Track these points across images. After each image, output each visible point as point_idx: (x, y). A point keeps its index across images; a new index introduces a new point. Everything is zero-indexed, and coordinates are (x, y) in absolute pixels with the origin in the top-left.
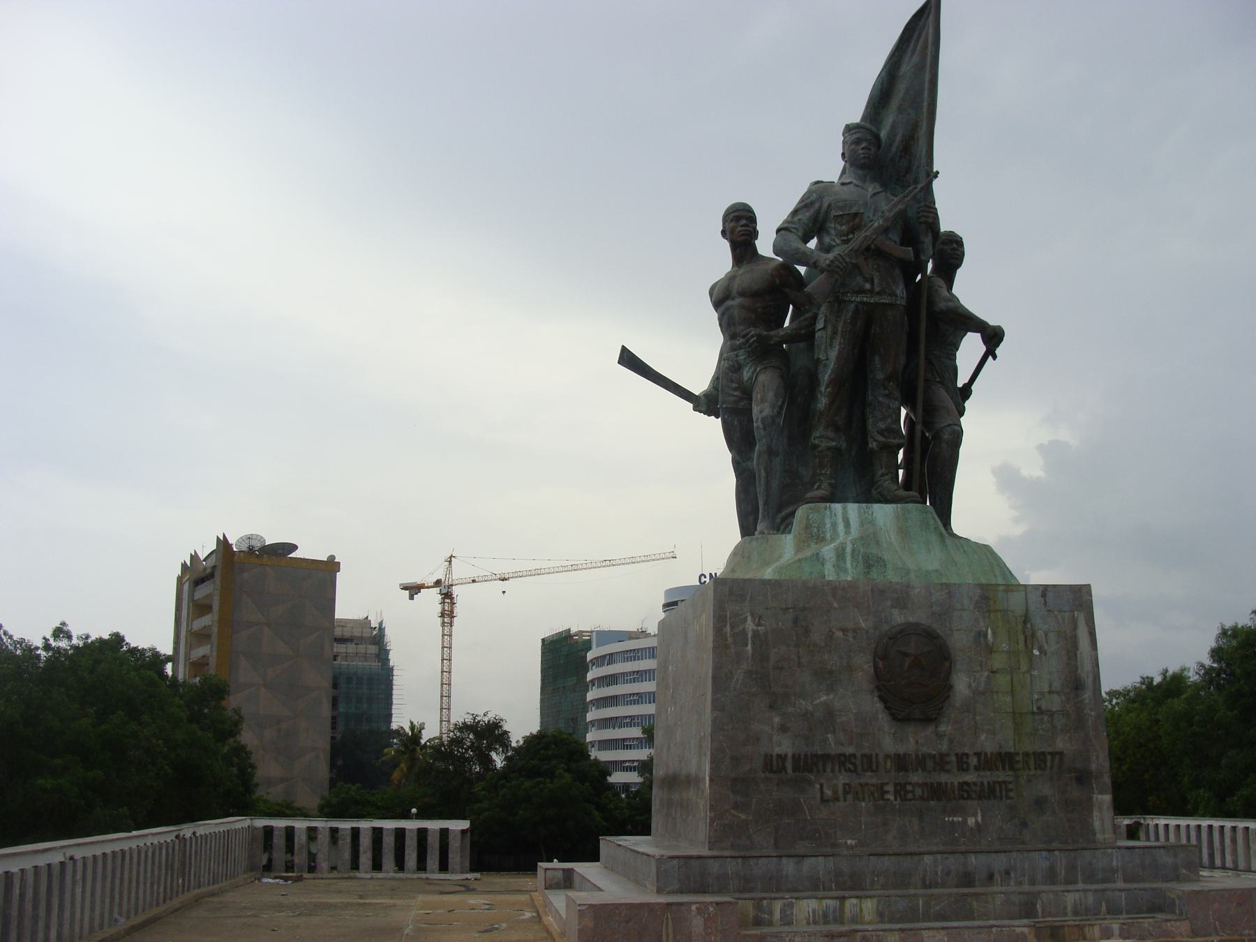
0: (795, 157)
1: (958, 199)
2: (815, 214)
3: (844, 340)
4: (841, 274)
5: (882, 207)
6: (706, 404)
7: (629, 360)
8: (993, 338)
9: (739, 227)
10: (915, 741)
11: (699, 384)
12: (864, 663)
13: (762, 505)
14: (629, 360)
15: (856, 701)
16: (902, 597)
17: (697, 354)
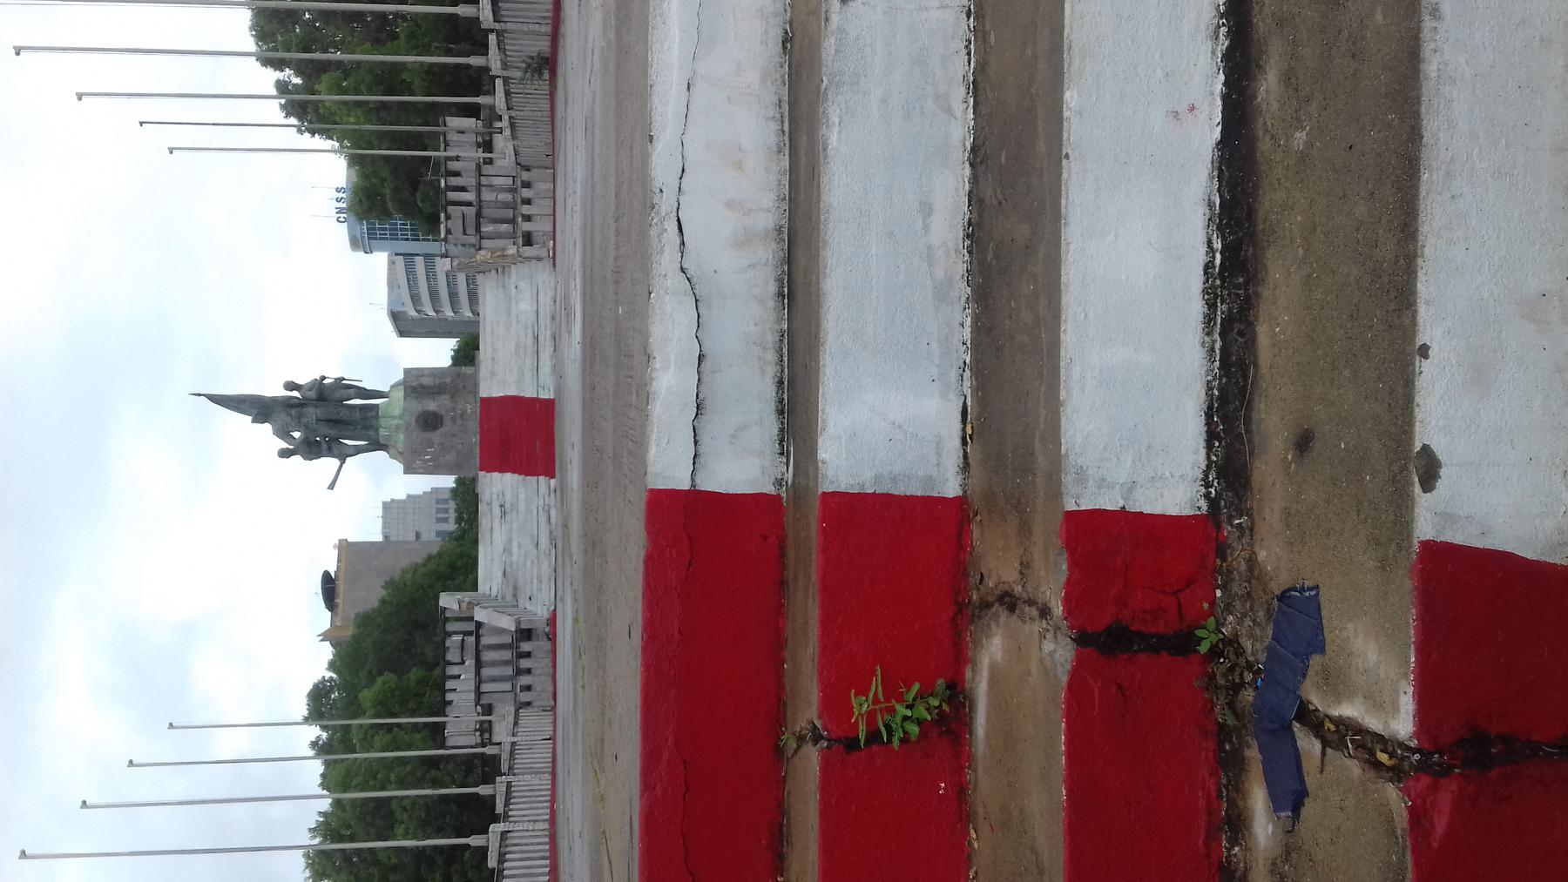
1: (276, 390)
2: (283, 433)
3: (322, 420)
4: (306, 428)
5: (283, 417)
6: (343, 462)
7: (331, 487)
8: (324, 378)
9: (285, 454)
10: (447, 421)
11: (335, 462)
12: (426, 435)
13: (376, 445)
14: (331, 487)
15: (436, 436)
17: (328, 464)
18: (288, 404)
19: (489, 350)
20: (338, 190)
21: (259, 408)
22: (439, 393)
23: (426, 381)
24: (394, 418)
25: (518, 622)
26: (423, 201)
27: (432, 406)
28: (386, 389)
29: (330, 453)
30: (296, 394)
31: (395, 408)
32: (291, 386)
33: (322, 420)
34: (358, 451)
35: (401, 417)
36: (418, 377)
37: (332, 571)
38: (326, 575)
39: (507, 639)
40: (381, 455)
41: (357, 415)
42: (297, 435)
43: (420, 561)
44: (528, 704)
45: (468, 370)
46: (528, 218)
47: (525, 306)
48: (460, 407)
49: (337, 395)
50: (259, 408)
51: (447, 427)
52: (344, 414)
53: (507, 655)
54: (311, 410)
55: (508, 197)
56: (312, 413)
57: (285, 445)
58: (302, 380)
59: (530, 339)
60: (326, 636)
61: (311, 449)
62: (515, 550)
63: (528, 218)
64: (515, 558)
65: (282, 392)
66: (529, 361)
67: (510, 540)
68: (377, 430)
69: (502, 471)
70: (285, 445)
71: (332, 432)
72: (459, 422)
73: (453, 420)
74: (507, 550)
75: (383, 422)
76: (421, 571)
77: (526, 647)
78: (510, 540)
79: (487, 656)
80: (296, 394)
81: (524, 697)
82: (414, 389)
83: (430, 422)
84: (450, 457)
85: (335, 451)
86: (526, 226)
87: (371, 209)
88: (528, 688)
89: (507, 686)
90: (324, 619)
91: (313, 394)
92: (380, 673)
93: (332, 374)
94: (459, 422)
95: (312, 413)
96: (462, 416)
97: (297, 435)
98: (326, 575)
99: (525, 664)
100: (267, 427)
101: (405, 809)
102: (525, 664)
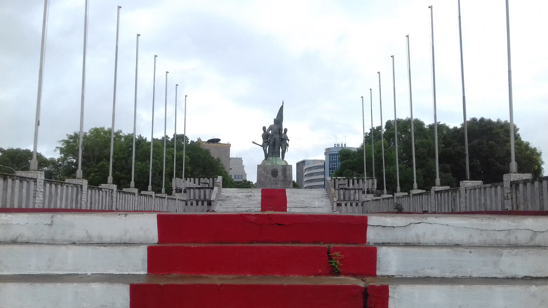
0: (269, 122)
1: (285, 125)
2: (271, 128)
3: (275, 140)
4: (272, 135)
5: (276, 128)
7: (253, 142)
8: (288, 140)
9: (264, 128)
10: (274, 179)
11: (261, 144)
12: (270, 172)
13: (267, 156)
14: (253, 142)
15: (270, 175)
16: (274, 166)
17: (261, 142)
18: (280, 129)
19: (301, 192)
20: (345, 144)
21: (279, 120)
22: (284, 176)
23: (288, 172)
24: (276, 162)
25: (213, 201)
26: (347, 172)
27: (280, 174)
28: (285, 159)
29: (264, 142)
30: (283, 132)
31: (279, 162)
32: (286, 130)
33: (275, 140)
34: (265, 151)
35: (276, 164)
36: (289, 169)
37: (220, 142)
38: (219, 140)
39: (207, 198)
40: (264, 158)
41: (276, 150)
42: (270, 132)
43: (225, 170)
44: (186, 204)
45: (292, 185)
46: (346, 205)
47: (317, 204)
48: (280, 183)
49: (283, 145)
50: (279, 120)
51: (273, 179)
52: (277, 147)
53: (202, 197)
54: (278, 137)
55: (352, 199)
56: (277, 136)
57: (267, 128)
58: (287, 134)
59: (306, 205)
60: (199, 140)
61: (266, 136)
62: (236, 200)
63: (346, 205)
64: (233, 200)
65: (284, 128)
66: (299, 205)
67: (239, 198)
68: (271, 156)
69: (262, 196)
70: (267, 128)
71: (271, 143)
72: (275, 182)
73: (275, 181)
74: (236, 197)
75: (274, 158)
76: (223, 170)
77: (205, 203)
78: (239, 198)
79: (202, 191)
80: (283, 132)
81: (189, 203)
82: (285, 168)
83: (275, 173)
84: (263, 180)
85: (265, 144)
86: (343, 204)
87: (343, 155)
88: (192, 204)
89: (192, 198)
90: (205, 139)
91: (283, 137)
92: (190, 157)
93: (290, 143)
94: (275, 182)
95: (277, 136)
96: (276, 183)
97: (270, 132)
98: (219, 140)
99: (200, 203)
100: (273, 123)
101: (146, 165)
102: (200, 203)
